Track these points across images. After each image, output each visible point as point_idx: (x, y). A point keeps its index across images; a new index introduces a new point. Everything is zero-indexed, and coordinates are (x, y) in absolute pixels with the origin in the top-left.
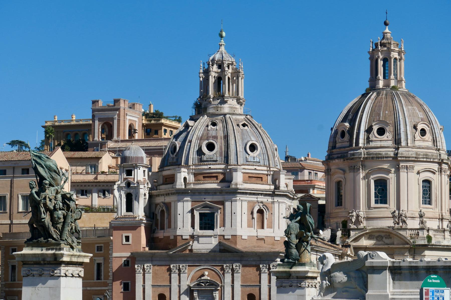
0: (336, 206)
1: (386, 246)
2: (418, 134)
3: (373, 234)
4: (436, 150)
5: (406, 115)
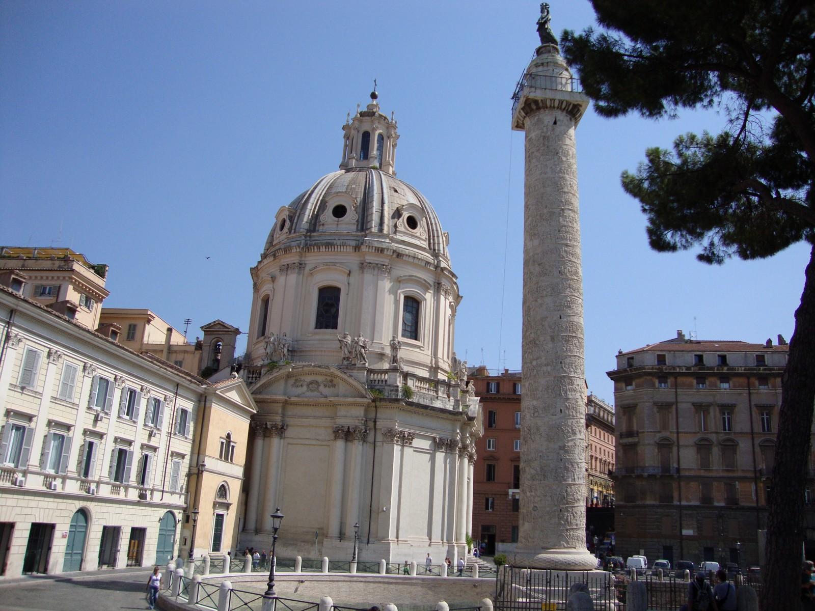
0: (258, 338)
1: (323, 400)
2: (402, 223)
3: (302, 378)
4: (432, 256)
5: (386, 196)
